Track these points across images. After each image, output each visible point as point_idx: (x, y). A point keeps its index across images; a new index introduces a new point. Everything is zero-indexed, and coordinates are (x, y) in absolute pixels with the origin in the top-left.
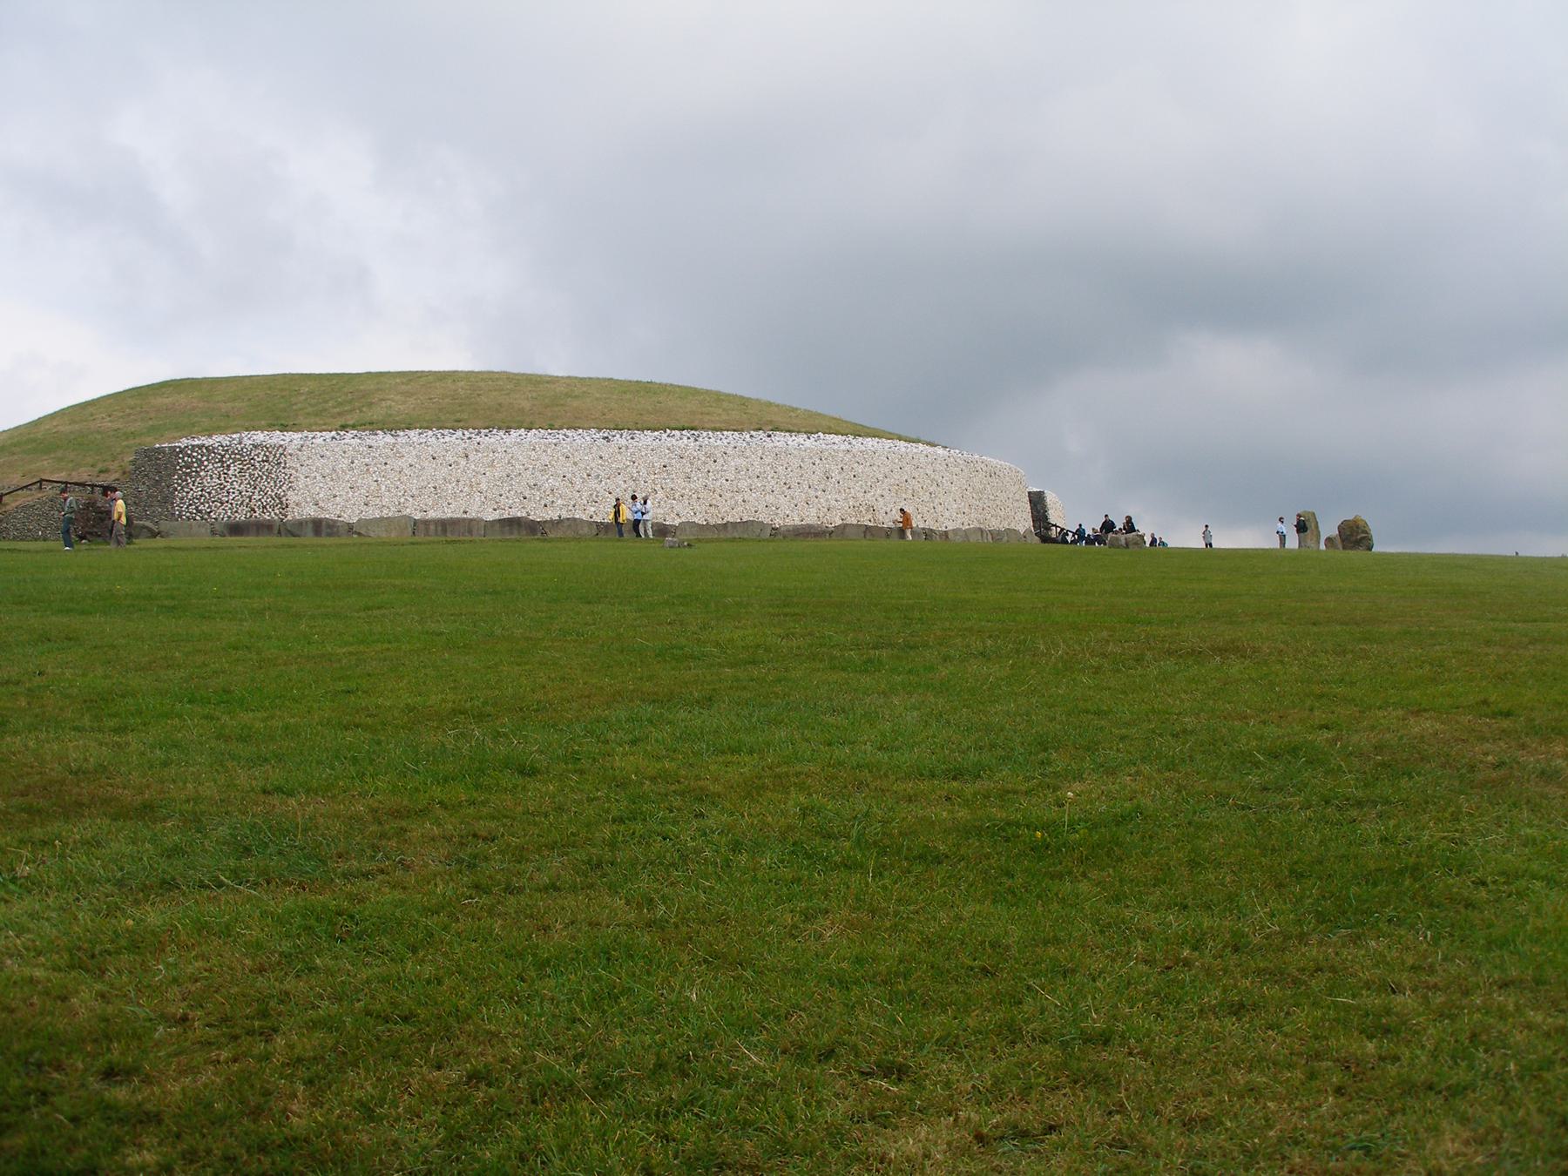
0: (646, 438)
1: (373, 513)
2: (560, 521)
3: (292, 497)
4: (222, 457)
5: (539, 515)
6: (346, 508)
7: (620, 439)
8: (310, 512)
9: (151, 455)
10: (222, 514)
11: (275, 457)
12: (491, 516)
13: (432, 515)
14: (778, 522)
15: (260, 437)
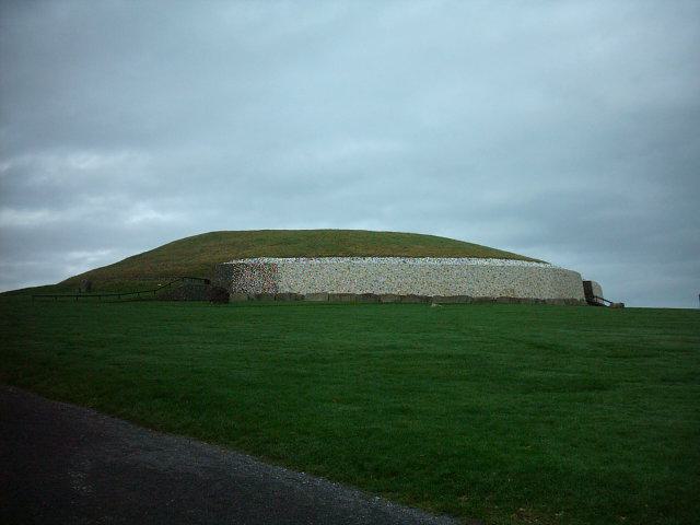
0: (420, 261)
1: (312, 291)
2: (387, 295)
3: (280, 285)
4: (252, 268)
5: (378, 293)
6: (301, 288)
7: (410, 261)
8: (288, 290)
9: (223, 267)
10: (252, 291)
11: (273, 268)
12: (358, 292)
13: (335, 292)
14: (474, 296)
15: (266, 260)
